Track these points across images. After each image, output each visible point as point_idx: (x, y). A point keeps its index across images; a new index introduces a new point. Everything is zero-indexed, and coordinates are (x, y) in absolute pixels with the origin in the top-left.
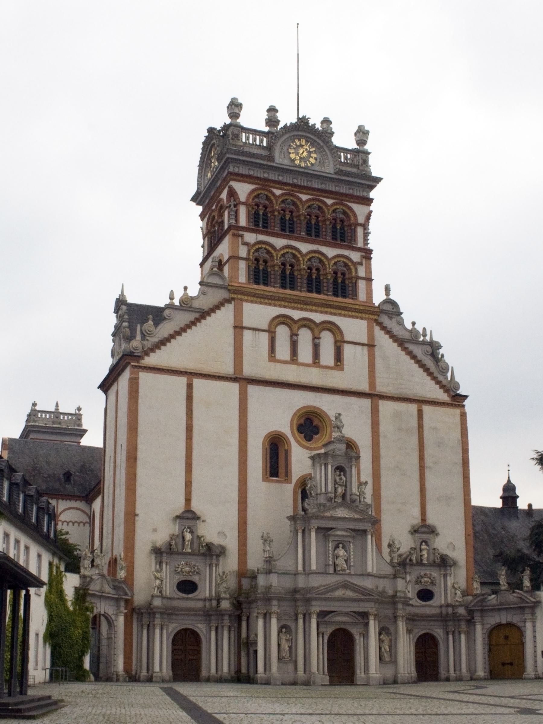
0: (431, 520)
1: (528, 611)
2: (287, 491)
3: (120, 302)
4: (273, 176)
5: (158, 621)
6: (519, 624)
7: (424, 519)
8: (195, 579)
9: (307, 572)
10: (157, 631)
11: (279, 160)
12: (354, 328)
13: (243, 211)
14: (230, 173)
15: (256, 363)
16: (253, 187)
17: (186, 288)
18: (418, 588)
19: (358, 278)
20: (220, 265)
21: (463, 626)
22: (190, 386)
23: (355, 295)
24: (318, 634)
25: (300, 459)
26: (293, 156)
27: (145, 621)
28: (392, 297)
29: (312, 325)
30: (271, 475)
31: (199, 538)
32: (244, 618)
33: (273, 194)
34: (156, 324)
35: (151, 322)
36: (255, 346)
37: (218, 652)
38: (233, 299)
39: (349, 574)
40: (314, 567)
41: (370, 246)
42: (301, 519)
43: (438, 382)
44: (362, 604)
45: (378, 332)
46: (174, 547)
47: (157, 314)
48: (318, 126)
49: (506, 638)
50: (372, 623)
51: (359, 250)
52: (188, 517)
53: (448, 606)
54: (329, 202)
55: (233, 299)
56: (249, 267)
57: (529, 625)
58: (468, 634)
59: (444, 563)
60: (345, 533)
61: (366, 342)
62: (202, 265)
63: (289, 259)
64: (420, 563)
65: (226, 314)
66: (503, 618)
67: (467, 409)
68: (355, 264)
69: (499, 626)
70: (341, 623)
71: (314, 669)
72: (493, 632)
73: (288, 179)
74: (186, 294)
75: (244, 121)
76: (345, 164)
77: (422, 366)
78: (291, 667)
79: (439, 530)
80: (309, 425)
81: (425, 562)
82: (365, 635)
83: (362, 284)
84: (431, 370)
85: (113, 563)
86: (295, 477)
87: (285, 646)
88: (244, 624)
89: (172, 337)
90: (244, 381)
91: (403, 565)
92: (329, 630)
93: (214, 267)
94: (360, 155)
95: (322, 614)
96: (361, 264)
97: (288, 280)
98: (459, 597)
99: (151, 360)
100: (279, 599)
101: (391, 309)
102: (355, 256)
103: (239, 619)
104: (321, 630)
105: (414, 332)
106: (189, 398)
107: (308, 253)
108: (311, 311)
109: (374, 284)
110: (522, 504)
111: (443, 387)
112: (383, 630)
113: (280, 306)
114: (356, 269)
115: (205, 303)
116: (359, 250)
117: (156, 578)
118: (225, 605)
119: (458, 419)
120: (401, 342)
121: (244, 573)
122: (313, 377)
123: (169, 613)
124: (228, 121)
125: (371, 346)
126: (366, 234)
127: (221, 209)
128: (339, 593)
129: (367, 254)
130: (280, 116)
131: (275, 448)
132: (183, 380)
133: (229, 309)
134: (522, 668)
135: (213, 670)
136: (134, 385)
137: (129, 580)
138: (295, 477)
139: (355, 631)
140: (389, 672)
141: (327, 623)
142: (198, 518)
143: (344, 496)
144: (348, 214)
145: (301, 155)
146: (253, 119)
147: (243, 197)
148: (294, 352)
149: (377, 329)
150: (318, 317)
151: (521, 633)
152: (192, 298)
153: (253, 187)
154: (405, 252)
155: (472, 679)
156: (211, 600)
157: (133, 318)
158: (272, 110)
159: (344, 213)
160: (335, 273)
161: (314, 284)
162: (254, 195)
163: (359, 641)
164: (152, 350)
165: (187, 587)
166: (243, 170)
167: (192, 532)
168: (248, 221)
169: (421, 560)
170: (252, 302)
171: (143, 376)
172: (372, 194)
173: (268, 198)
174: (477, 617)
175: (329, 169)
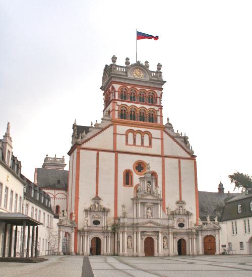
1: (217, 231)
2: (132, 189)
3: (74, 126)
4: (127, 82)
5: (86, 234)
6: (214, 236)
7: (181, 199)
8: (99, 220)
9: (137, 218)
11: (130, 76)
12: (156, 133)
13: (117, 94)
14: (112, 81)
16: (120, 86)
17: (97, 121)
18: (179, 223)
19: (158, 116)
20: (109, 112)
21: (195, 236)
22: (98, 154)
23: (156, 121)
25: (136, 178)
26: (135, 75)
27: (82, 234)
31: (100, 206)
32: (116, 233)
34: (86, 133)
36: (121, 140)
37: (107, 245)
38: (113, 124)
39: (152, 218)
40: (140, 216)
41: (162, 105)
42: (135, 200)
43: (186, 151)
45: (165, 134)
46: (92, 209)
47: (86, 129)
48: (143, 63)
49: (210, 240)
50: (160, 235)
51: (158, 106)
52: (97, 199)
53: (189, 229)
54: (147, 90)
57: (217, 236)
58: (196, 239)
59: (188, 214)
61: (160, 138)
62: (103, 111)
63: (133, 110)
64: (179, 214)
65: (111, 129)
66: (209, 233)
67: (197, 160)
68: (156, 111)
69: (207, 236)
70: (149, 235)
71: (140, 250)
72: (206, 238)
74: (97, 123)
75: (117, 63)
76: (154, 76)
77: (179, 144)
78: (132, 250)
80: (140, 167)
82: (158, 239)
83: (159, 118)
85: (71, 214)
86: (134, 185)
87: (130, 243)
88: (116, 235)
89: (92, 137)
91: (173, 214)
92: (145, 238)
93: (107, 113)
94: (159, 73)
95: (143, 232)
96: (159, 111)
97: (133, 117)
98: (193, 226)
99: (84, 146)
100: (128, 227)
101: (170, 126)
102: (156, 108)
103: (114, 234)
104: (142, 237)
105: (178, 134)
106: (98, 158)
109: (163, 118)
110: (226, 191)
111: (188, 153)
112: (164, 238)
113: (130, 126)
115: (103, 126)
116: (158, 106)
117: (86, 220)
118: (110, 229)
119: (193, 164)
120: (173, 138)
121: (116, 218)
123: (90, 232)
124: (112, 63)
125: (162, 139)
126: (161, 101)
127: (110, 93)
129: (161, 107)
130: (130, 61)
131: (128, 174)
132: (95, 152)
133: (111, 128)
134: (215, 251)
136: (78, 153)
138: (134, 185)
139: (154, 238)
140: (166, 252)
141: (144, 235)
142: (100, 199)
143: (150, 192)
144: (154, 93)
145: (136, 74)
146: (121, 62)
147: (117, 90)
149: (164, 133)
150: (143, 130)
151: (214, 239)
152: (99, 124)
153: (120, 86)
154: (174, 108)
156: (104, 227)
157: (79, 131)
158: (127, 59)
159: (153, 93)
160: (150, 114)
161: (142, 118)
162: (121, 88)
163: (155, 241)
164: (85, 142)
165: (96, 223)
167: (98, 204)
169: (180, 213)
171: (81, 151)
172: (163, 87)
173: (126, 89)
174: (200, 233)
175: (148, 79)
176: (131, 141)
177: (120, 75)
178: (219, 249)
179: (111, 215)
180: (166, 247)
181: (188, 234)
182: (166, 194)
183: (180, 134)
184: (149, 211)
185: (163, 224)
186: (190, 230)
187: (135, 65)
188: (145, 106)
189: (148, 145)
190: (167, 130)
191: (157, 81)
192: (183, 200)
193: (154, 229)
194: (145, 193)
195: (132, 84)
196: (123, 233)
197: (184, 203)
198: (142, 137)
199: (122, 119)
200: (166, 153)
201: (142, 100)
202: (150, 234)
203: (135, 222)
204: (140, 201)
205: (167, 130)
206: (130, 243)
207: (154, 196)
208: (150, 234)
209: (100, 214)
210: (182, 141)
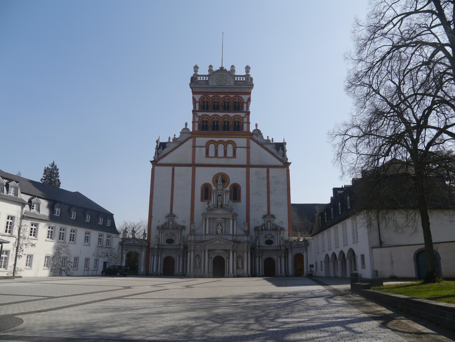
0: (272, 212)
4: (209, 90)
8: (173, 238)
10: (257, 259)
12: (241, 142)
13: (197, 105)
17: (175, 135)
18: (266, 239)
22: (173, 170)
28: (258, 128)
30: (205, 199)
33: (209, 97)
34: (163, 149)
35: (161, 149)
38: (192, 137)
40: (207, 233)
48: (228, 69)
50: (231, 254)
52: (171, 215)
54: (232, 96)
59: (278, 229)
60: (221, 219)
65: (190, 142)
66: (297, 251)
68: (243, 118)
73: (216, 90)
79: (276, 216)
81: (269, 229)
82: (229, 258)
83: (245, 125)
87: (198, 263)
90: (194, 165)
92: (213, 256)
95: (209, 251)
96: (245, 117)
99: (161, 161)
101: (258, 132)
104: (210, 256)
105: (268, 140)
108: (223, 137)
114: (243, 120)
119: (285, 172)
120: (261, 145)
122: (224, 161)
125: (248, 148)
129: (248, 113)
132: (171, 168)
135: (177, 271)
139: (225, 257)
142: (175, 216)
147: (197, 100)
150: (225, 140)
152: (177, 138)
158: (211, 66)
159: (239, 99)
164: (161, 158)
165: (170, 241)
166: (198, 90)
168: (199, 108)
170: (199, 137)
173: (208, 99)
176: (212, 153)
179: (186, 232)
180: (240, 266)
182: (251, 208)
183: (271, 140)
186: (279, 248)
187: (217, 71)
188: (229, 114)
189: (232, 155)
191: (247, 84)
192: (272, 212)
194: (215, 207)
196: (190, 251)
197: (273, 217)
198: (215, 147)
199: (203, 130)
200: (252, 162)
201: (226, 108)
203: (204, 239)
205: (255, 137)
206: (198, 263)
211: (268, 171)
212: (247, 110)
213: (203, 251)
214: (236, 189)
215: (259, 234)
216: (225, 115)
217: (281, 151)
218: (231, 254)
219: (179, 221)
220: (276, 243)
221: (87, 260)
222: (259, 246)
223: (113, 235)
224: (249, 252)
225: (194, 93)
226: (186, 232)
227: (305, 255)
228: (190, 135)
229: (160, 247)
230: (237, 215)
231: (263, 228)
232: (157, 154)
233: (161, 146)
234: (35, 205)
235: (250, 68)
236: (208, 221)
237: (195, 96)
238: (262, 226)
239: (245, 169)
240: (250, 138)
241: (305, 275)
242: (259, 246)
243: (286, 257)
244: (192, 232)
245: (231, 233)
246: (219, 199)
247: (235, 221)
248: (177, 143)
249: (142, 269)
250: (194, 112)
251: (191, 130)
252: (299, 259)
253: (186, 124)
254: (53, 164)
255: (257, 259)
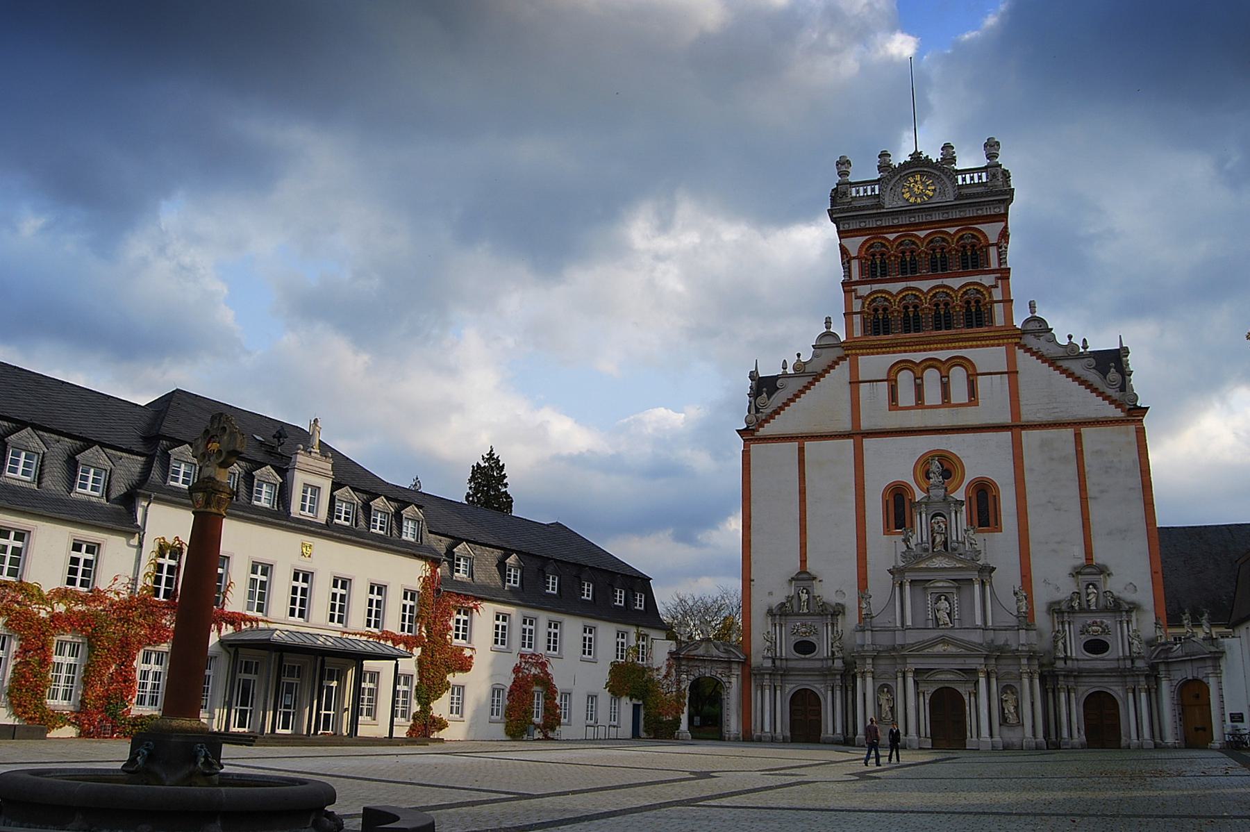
4: (886, 222)
5: (766, 682)
8: (813, 639)
10: (1063, 696)
12: (988, 357)
13: (855, 265)
15: (875, 413)
17: (799, 355)
22: (801, 450)
24: (917, 694)
26: (907, 196)
29: (939, 365)
34: (770, 395)
35: (765, 395)
38: (847, 355)
40: (909, 623)
44: (968, 661)
45: (1022, 357)
48: (935, 156)
50: (982, 681)
51: (993, 272)
52: (804, 577)
54: (952, 230)
55: (847, 355)
56: (864, 319)
59: (1120, 608)
60: (946, 584)
64: (1085, 610)
65: (842, 372)
66: (1188, 672)
68: (989, 289)
73: (904, 220)
79: (1112, 570)
81: (1093, 608)
82: (976, 695)
83: (998, 309)
84: (1095, 386)
87: (886, 707)
89: (786, 404)
90: (858, 435)
94: (994, 170)
95: (917, 672)
96: (996, 286)
97: (912, 322)
99: (765, 431)
101: (1039, 327)
107: (899, 293)
108: (936, 349)
111: (1112, 402)
113: (900, 352)
114: (991, 296)
116: (993, 272)
119: (1133, 437)
120: (1052, 362)
122: (943, 418)
123: (779, 672)
125: (1012, 373)
128: (940, 648)
129: (1004, 274)
131: (898, 499)
133: (845, 365)
137: (745, 646)
139: (961, 689)
142: (815, 578)
143: (945, 544)
145: (918, 190)
147: (854, 253)
148: (919, 395)
155: (1156, 746)
156: (827, 659)
158: (884, 155)
159: (974, 236)
161: (943, 319)
164: (767, 421)
165: (805, 647)
166: (854, 225)
168: (862, 273)
173: (883, 245)
176: (906, 396)
177: (860, 209)
178: (1220, 730)
179: (850, 620)
180: (1012, 719)
181: (1120, 674)
184: (944, 604)
185: (1000, 642)
186: (1128, 664)
188: (948, 282)
190: (1030, 341)
192: (1098, 558)
193: (959, 661)
194: (926, 550)
195: (901, 226)
197: (1103, 570)
200: (1027, 415)
201: (939, 266)
202: (949, 677)
203: (899, 641)
204: (909, 576)
205: (1030, 341)
206: (886, 707)
207: (961, 560)
208: (949, 677)
209: (817, 623)
210: (1088, 367)
211: (1078, 437)
212: (1000, 264)
213: (900, 675)
214: (983, 493)
215: (1063, 623)
216: (938, 287)
217: (1113, 375)
218: (982, 681)
219: (827, 592)
220: (1117, 650)
221: (592, 698)
222: (1066, 659)
223: (653, 634)
224: (1036, 676)
225: (842, 234)
226: (850, 620)
227: (1212, 682)
228: (839, 352)
229: (778, 663)
230: (993, 569)
231: (1076, 605)
232: (753, 411)
233: (763, 386)
234: (462, 562)
235: (998, 144)
236: (907, 587)
237: (846, 242)
238: (1072, 600)
239: (1007, 435)
240: (1016, 344)
241: (1217, 745)
242: (1066, 659)
243: (1153, 693)
244: (865, 621)
245: (979, 622)
246: (936, 527)
247: (988, 588)
248: (810, 374)
249: (733, 724)
250: (848, 285)
251: (843, 338)
252: (1194, 697)
253: (828, 322)
254: (491, 454)
255: (1063, 696)
